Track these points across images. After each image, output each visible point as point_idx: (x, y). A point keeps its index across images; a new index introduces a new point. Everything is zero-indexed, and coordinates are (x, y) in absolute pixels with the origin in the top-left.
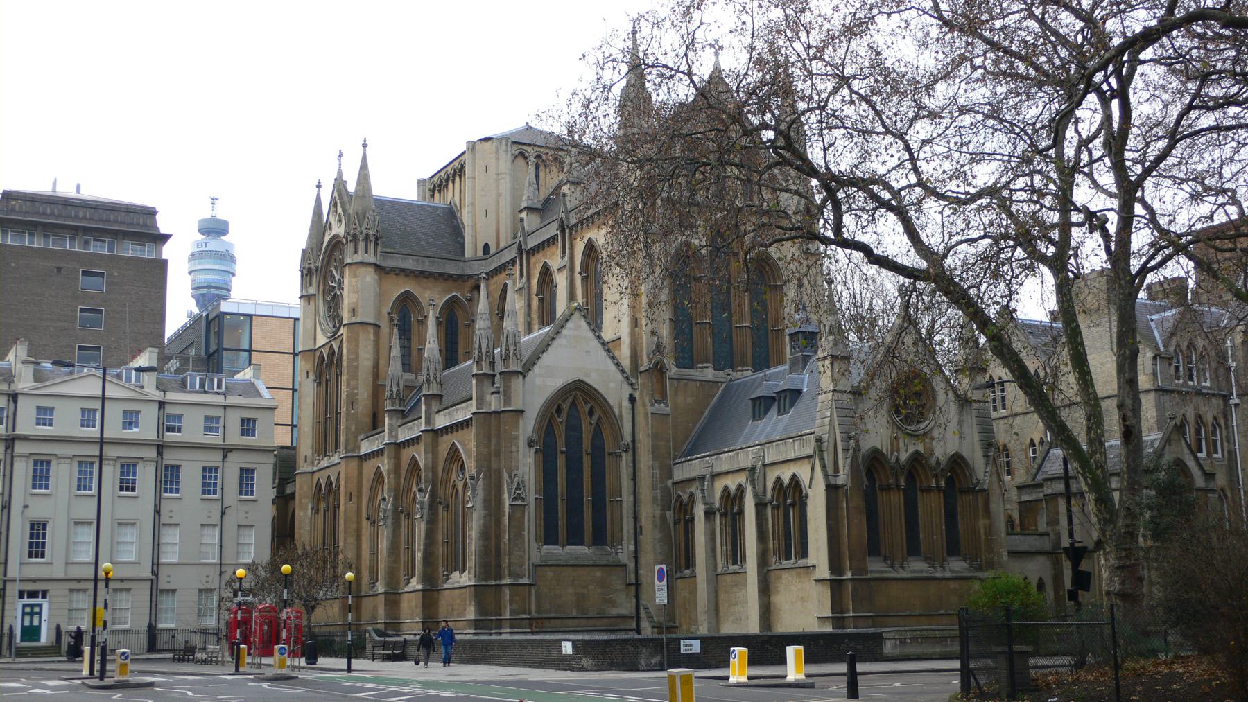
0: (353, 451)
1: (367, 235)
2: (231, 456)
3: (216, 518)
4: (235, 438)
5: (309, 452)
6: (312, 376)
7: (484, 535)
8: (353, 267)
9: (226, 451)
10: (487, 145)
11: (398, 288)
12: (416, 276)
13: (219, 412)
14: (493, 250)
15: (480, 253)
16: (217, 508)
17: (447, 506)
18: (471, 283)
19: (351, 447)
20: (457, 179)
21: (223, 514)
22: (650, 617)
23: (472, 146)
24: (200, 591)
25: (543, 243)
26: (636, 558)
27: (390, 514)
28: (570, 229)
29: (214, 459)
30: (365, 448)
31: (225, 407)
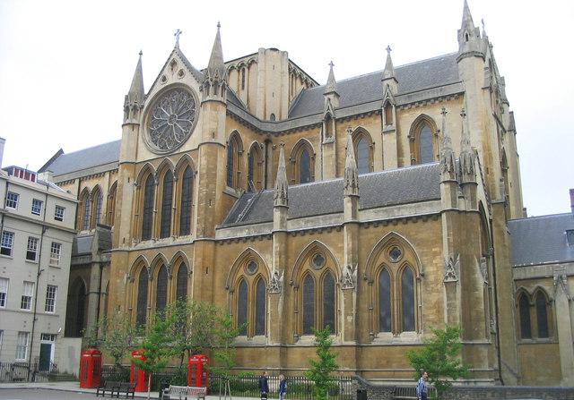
0: (211, 236)
1: (216, 82)
2: (48, 233)
3: (34, 279)
4: (50, 219)
5: (127, 237)
6: (132, 181)
7: (463, 304)
8: (214, 103)
9: (45, 227)
10: (275, 53)
11: (235, 127)
12: (240, 122)
13: (41, 198)
14: (277, 119)
15: (268, 119)
16: (35, 269)
17: (372, 282)
18: (265, 136)
19: (208, 232)
20: (234, 73)
21: (39, 274)
22: (511, 371)
23: (264, 51)
24: (20, 332)
25: (359, 115)
26: (497, 329)
27: (282, 285)
28: (397, 107)
29: (36, 232)
30: (221, 235)
31: (47, 195)
